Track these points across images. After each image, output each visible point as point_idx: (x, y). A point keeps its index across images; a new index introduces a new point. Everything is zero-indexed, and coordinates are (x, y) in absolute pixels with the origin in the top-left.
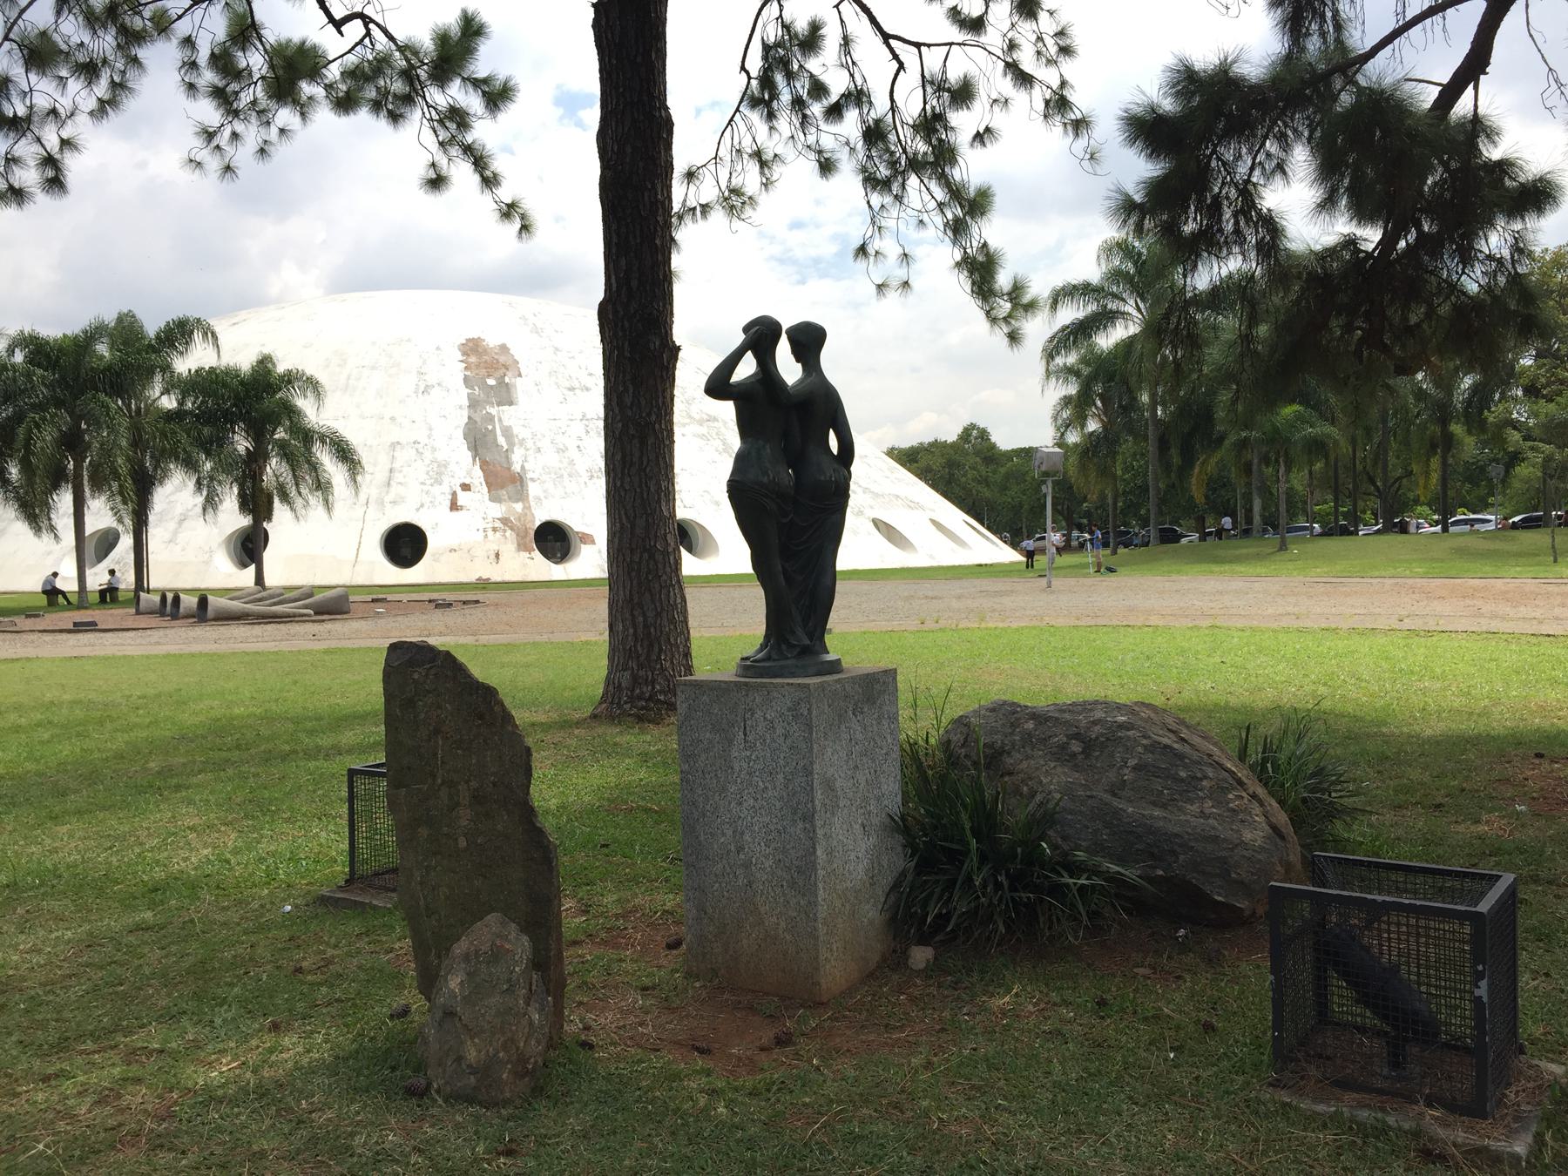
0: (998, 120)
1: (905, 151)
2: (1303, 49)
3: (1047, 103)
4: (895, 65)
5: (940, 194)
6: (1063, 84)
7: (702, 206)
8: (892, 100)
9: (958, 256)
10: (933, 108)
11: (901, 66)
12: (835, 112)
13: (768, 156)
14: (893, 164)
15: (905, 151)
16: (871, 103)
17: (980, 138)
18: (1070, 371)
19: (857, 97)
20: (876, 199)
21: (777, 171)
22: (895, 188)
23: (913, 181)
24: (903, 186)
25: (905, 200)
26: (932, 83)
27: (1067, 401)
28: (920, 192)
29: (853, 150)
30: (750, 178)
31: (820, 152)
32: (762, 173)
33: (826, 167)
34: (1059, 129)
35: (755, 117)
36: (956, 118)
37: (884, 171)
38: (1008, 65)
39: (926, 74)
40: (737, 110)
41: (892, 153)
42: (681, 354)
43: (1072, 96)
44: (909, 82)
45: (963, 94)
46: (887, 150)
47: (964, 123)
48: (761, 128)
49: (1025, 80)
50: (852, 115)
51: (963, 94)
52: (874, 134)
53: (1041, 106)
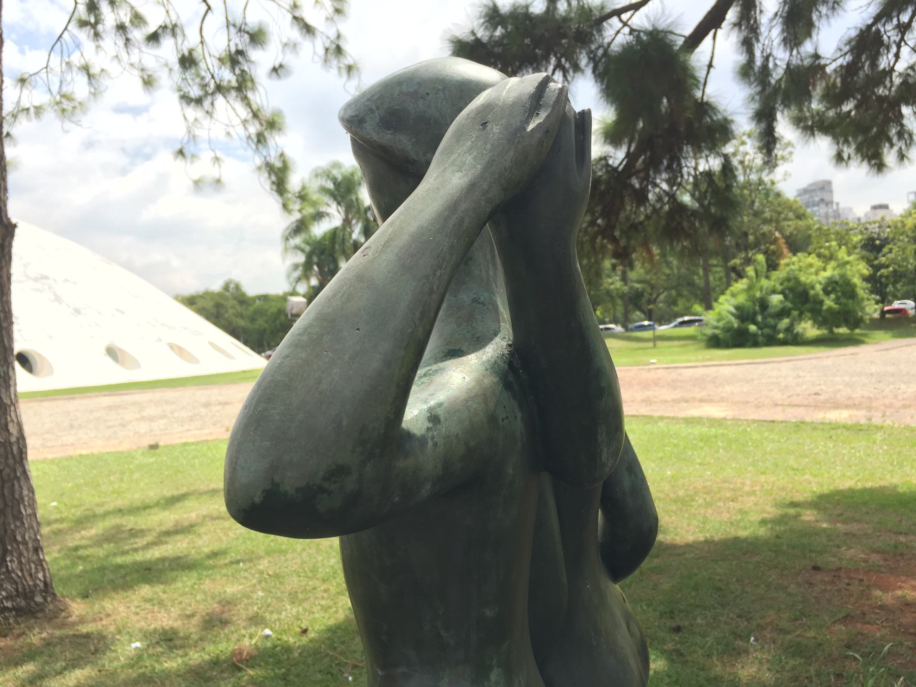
0: (289, 59)
1: (213, 77)
2: (555, 8)
3: (327, 50)
4: (205, 8)
5: (244, 113)
6: (339, 36)
7: (36, 108)
8: (202, 37)
9: (258, 161)
10: (237, 45)
11: (209, 8)
12: (154, 38)
13: (95, 70)
14: (204, 86)
15: (213, 77)
16: (184, 35)
17: (276, 70)
18: (297, 248)
19: (173, 29)
20: (192, 112)
21: (105, 82)
22: (207, 103)
23: (220, 100)
24: (212, 104)
25: (215, 116)
26: (234, 25)
27: (296, 267)
28: (228, 110)
29: (171, 70)
30: (79, 87)
31: (143, 70)
32: (90, 83)
33: (148, 82)
34: (334, 71)
35: (83, 35)
36: (254, 54)
37: (195, 92)
38: (295, 18)
39: (229, 18)
40: (66, 29)
41: (203, 78)
42: (17, 231)
43: (345, 47)
44: (216, 20)
45: (257, 37)
46: (198, 75)
47: (261, 60)
48: (88, 45)
49: (308, 29)
50: (167, 43)
51: (257, 37)
52: (187, 61)
53: (321, 52)
